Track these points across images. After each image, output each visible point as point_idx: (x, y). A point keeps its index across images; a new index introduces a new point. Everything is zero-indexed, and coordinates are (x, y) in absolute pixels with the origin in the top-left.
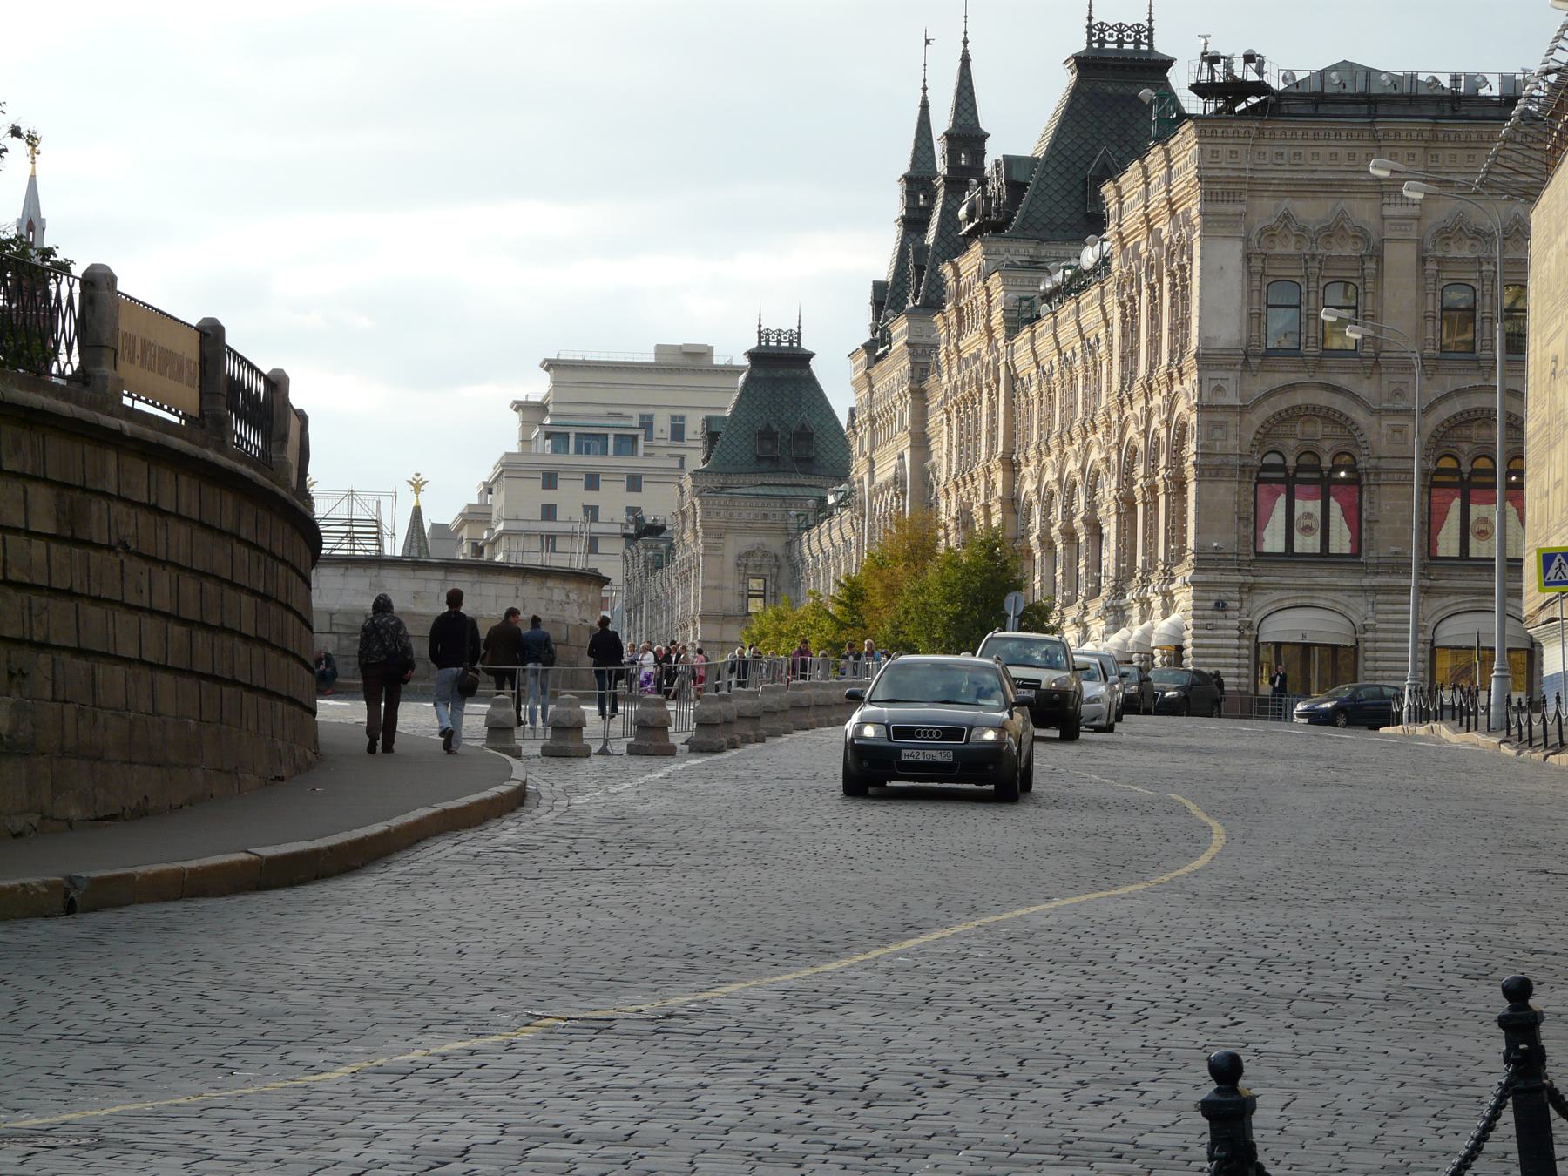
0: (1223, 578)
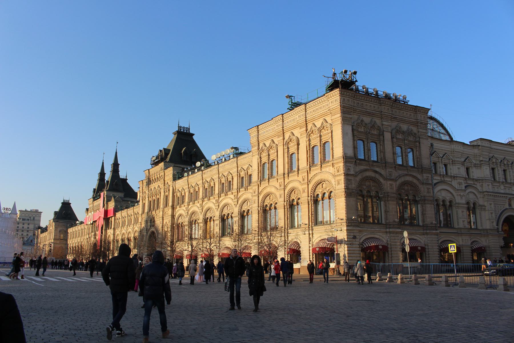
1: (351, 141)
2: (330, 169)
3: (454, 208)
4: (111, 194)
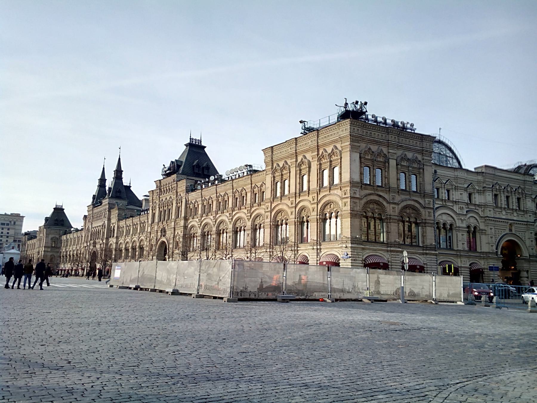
0: (357, 246)
1: (358, 168)
2: (338, 192)
3: (454, 232)
4: (114, 201)
